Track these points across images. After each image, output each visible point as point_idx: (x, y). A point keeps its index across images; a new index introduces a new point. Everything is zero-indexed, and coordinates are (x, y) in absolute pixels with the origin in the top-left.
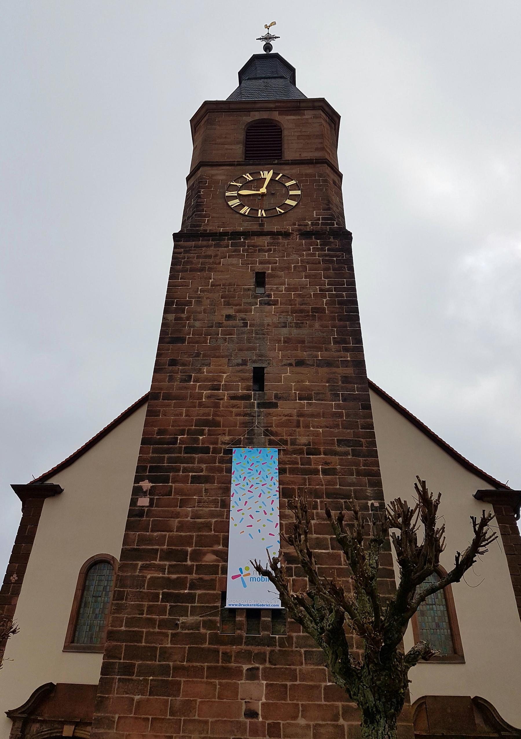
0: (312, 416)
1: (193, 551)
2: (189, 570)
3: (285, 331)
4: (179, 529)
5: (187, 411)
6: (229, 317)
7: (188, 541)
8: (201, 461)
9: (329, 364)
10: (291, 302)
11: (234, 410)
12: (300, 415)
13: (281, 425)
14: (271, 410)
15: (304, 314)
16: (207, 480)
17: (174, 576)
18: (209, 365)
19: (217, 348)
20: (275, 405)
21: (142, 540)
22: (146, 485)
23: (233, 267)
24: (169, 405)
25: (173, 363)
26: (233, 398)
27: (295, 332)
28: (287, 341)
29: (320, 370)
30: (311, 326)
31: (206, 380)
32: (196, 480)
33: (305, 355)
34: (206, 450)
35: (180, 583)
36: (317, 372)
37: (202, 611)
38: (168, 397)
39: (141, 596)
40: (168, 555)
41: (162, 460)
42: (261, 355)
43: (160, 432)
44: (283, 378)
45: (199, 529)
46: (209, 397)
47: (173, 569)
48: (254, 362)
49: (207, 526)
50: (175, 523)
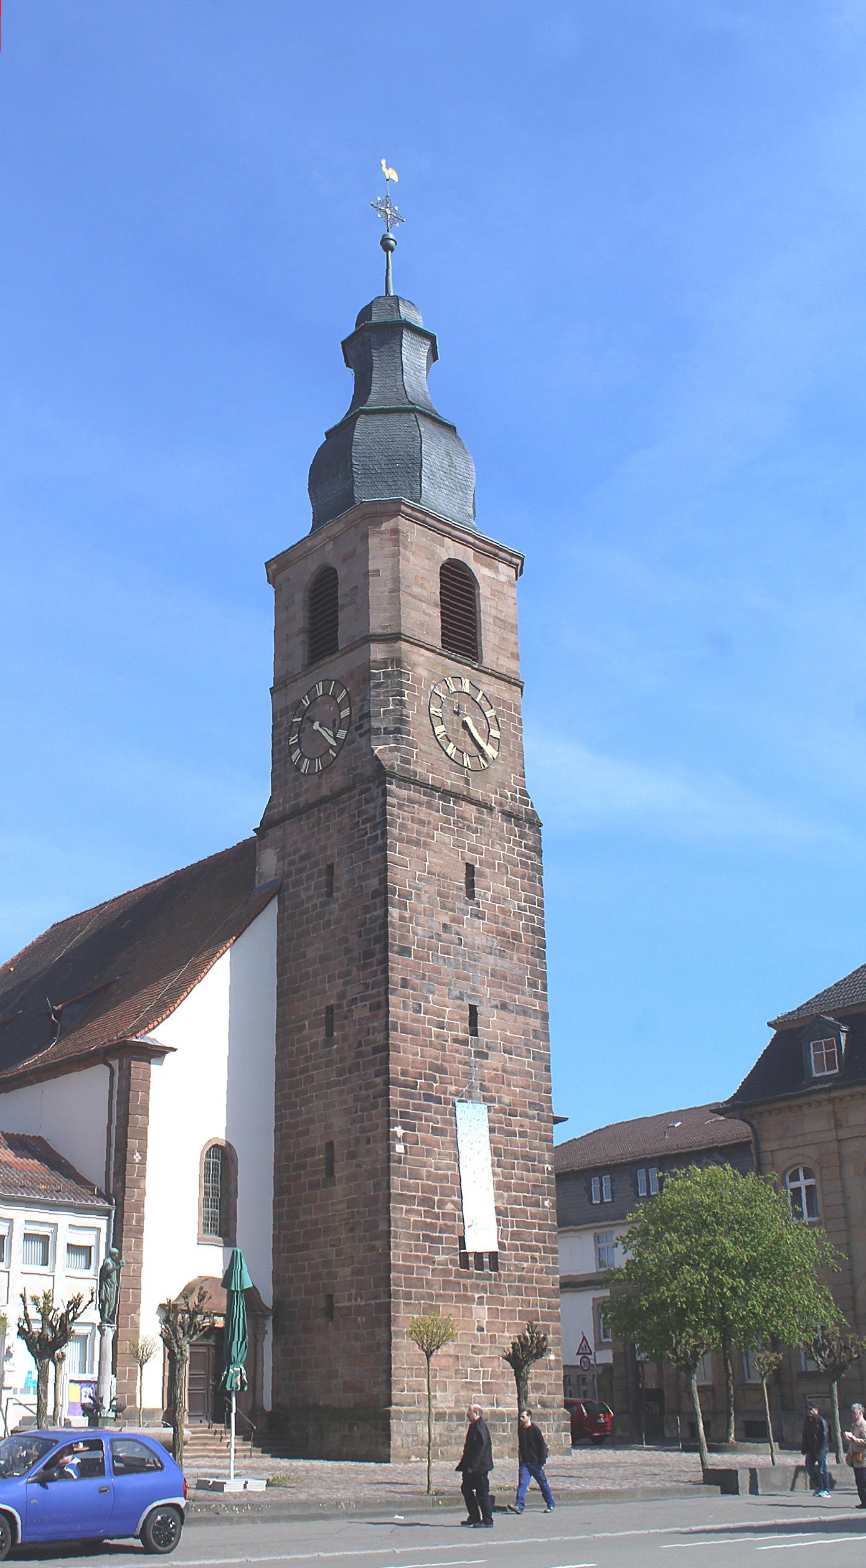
9: (525, 1012)
12: (504, 1071)
19: (437, 971)
20: (484, 1056)
26: (456, 1040)
31: (434, 1013)
36: (515, 1021)
42: (474, 990)
44: (492, 1021)
46: (438, 1036)
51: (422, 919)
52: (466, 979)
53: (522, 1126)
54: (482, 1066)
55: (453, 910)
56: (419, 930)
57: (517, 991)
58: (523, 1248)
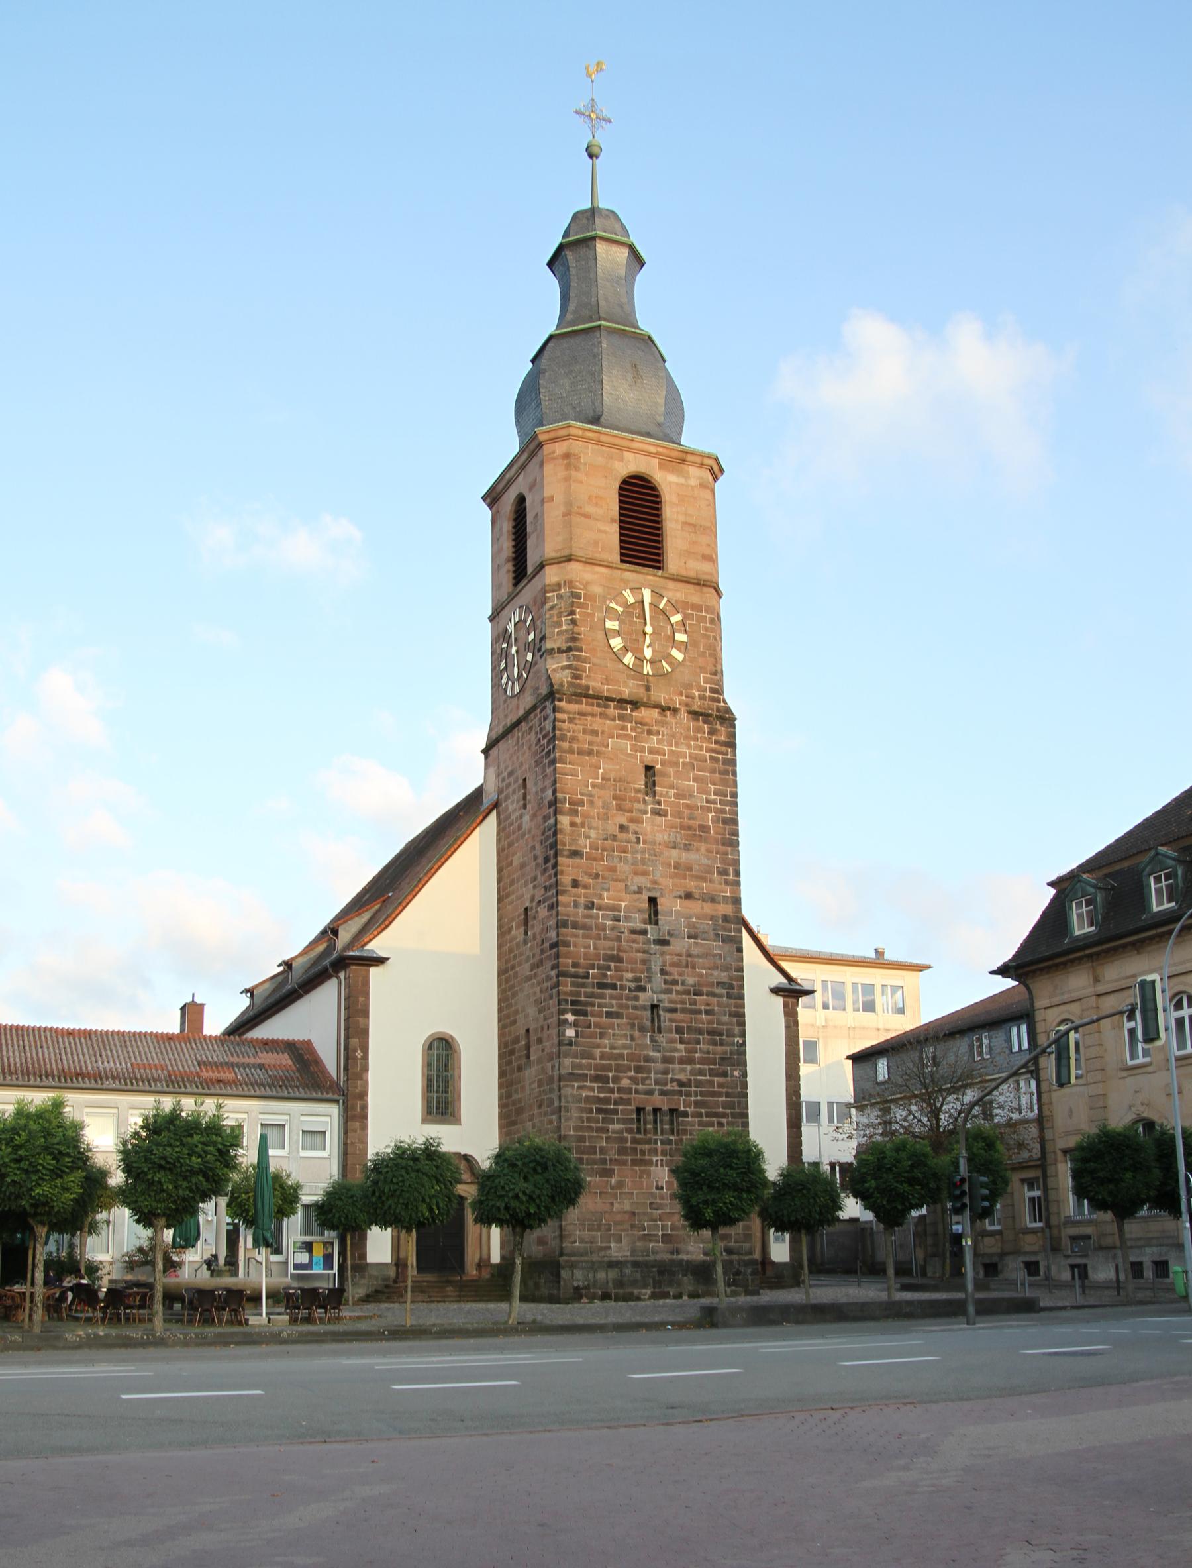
0: (698, 956)
1: (614, 1077)
2: (612, 1091)
4: (602, 1058)
5: (595, 944)
7: (608, 1068)
8: (611, 997)
11: (635, 945)
12: (689, 955)
13: (673, 965)
14: (666, 948)
16: (617, 1015)
17: (602, 1095)
18: (608, 890)
19: (613, 869)
24: (577, 936)
26: (633, 932)
31: (608, 908)
32: (609, 1015)
35: (607, 1101)
37: (624, 1121)
40: (596, 1079)
41: (579, 994)
43: (575, 965)
45: (616, 1059)
46: (612, 928)
47: (600, 1090)
49: (621, 1056)
50: (597, 1052)
51: (595, 823)
52: (645, 873)
53: (708, 1004)
55: (630, 811)
56: (593, 833)
58: (708, 1115)
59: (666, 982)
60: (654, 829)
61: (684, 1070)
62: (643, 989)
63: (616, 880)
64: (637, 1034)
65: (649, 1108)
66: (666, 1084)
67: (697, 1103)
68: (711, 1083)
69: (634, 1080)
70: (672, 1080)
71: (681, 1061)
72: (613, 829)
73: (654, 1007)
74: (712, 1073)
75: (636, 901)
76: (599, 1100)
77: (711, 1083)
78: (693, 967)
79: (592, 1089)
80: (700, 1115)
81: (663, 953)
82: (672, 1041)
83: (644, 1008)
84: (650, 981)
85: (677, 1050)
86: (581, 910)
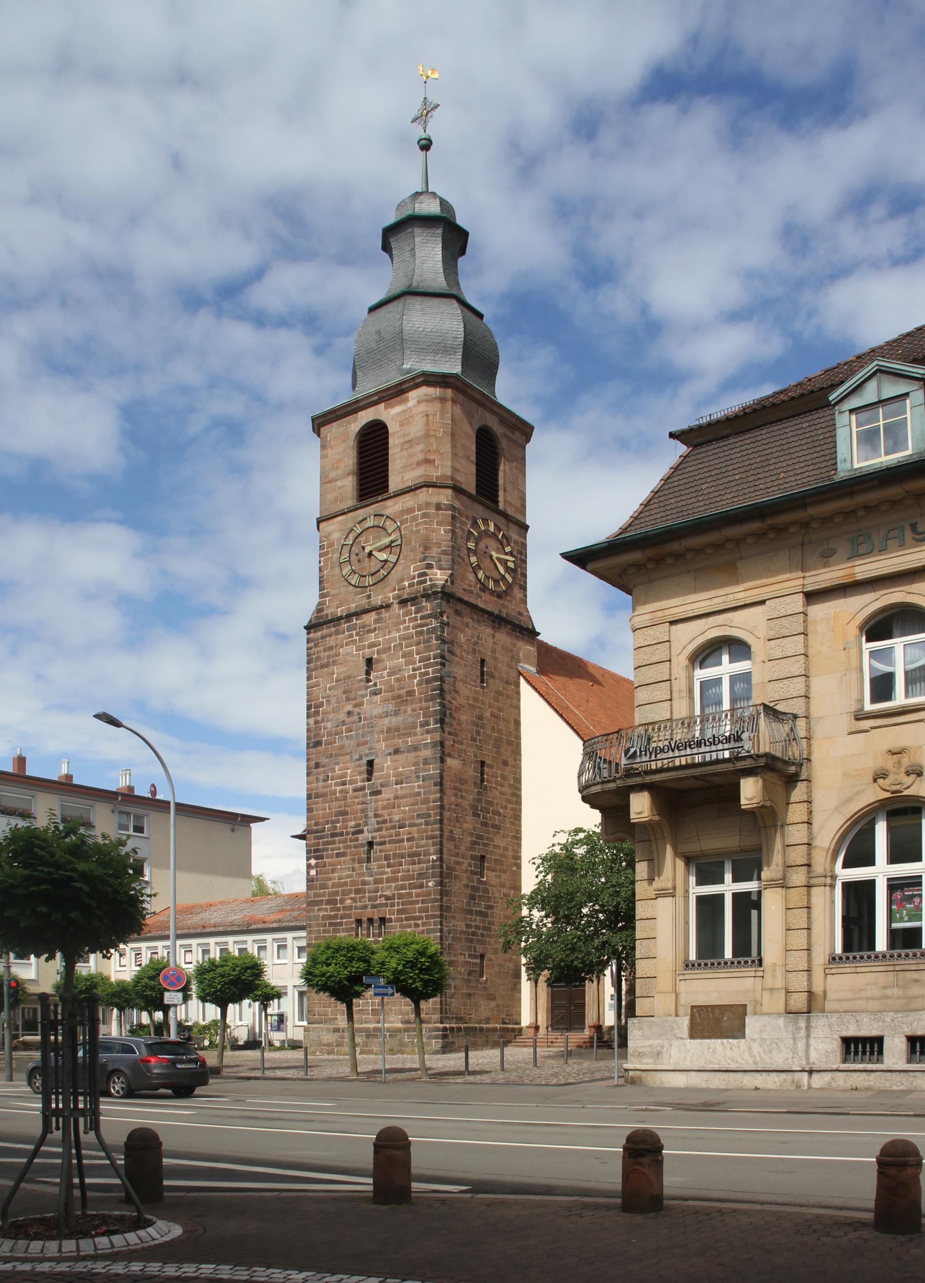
0: (403, 797)
2: (339, 909)
3: (387, 721)
6: (349, 713)
7: (337, 893)
8: (340, 842)
9: (415, 748)
10: (391, 689)
11: (356, 800)
13: (384, 808)
14: (379, 797)
15: (402, 699)
16: (343, 854)
18: (338, 764)
21: (316, 895)
22: (313, 862)
23: (350, 652)
24: (317, 803)
25: (317, 766)
26: (355, 790)
27: (394, 719)
28: (389, 730)
29: (409, 755)
30: (405, 712)
32: (338, 855)
33: (399, 742)
34: (342, 834)
35: (335, 917)
36: (407, 758)
38: (317, 796)
39: (319, 925)
40: (329, 902)
41: (318, 844)
43: (316, 824)
44: (386, 766)
46: (341, 792)
48: (367, 755)
49: (346, 884)
52: (365, 743)
53: (409, 834)
54: (376, 801)
55: (355, 699)
57: (409, 735)
58: (407, 919)
59: (378, 823)
60: (373, 706)
61: (390, 887)
62: (361, 832)
63: (344, 755)
64: (357, 865)
65: (365, 919)
66: (376, 900)
67: (399, 912)
68: (410, 895)
69: (353, 899)
70: (381, 896)
71: (389, 880)
72: (342, 716)
73: (371, 844)
74: (412, 887)
75: (358, 766)
76: (331, 917)
77: (410, 895)
78: (399, 807)
79: (326, 910)
80: (401, 920)
81: (376, 801)
82: (383, 866)
83: (362, 845)
84: (366, 824)
85: (385, 873)
86: (321, 784)
